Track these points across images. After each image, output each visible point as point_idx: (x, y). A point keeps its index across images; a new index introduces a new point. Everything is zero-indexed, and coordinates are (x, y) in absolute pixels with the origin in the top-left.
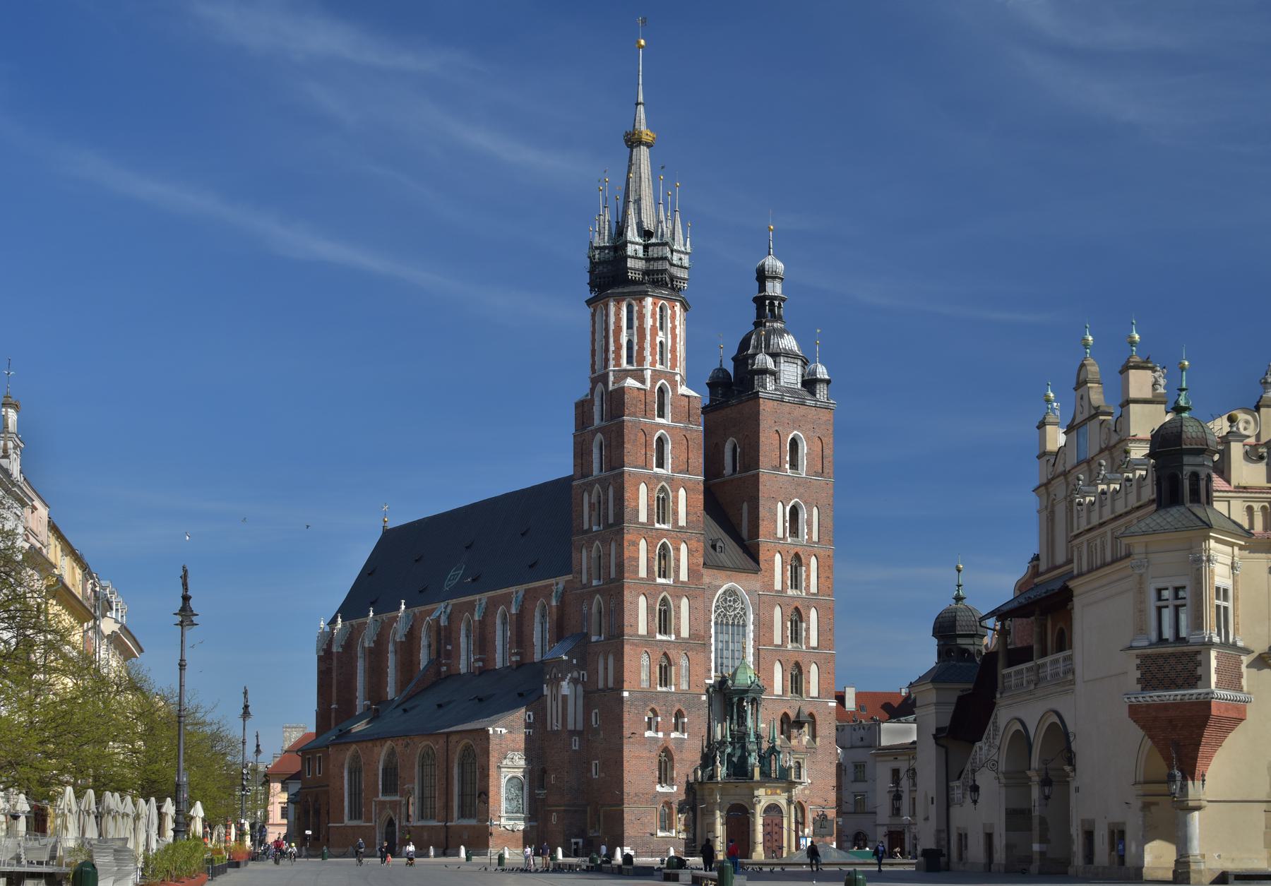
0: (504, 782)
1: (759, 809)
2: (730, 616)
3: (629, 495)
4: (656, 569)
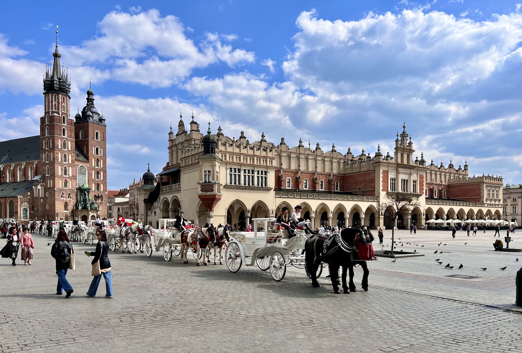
4: (63, 160)
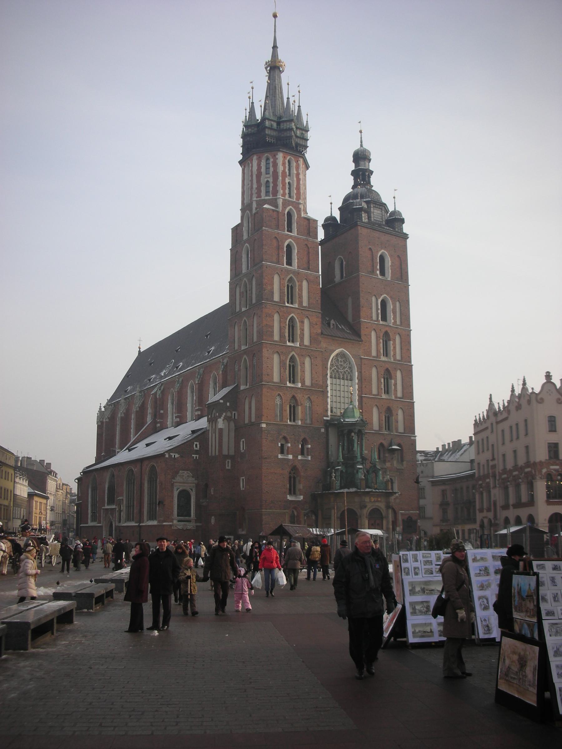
0: (176, 493)
2: (341, 372)
3: (266, 281)
4: (287, 335)
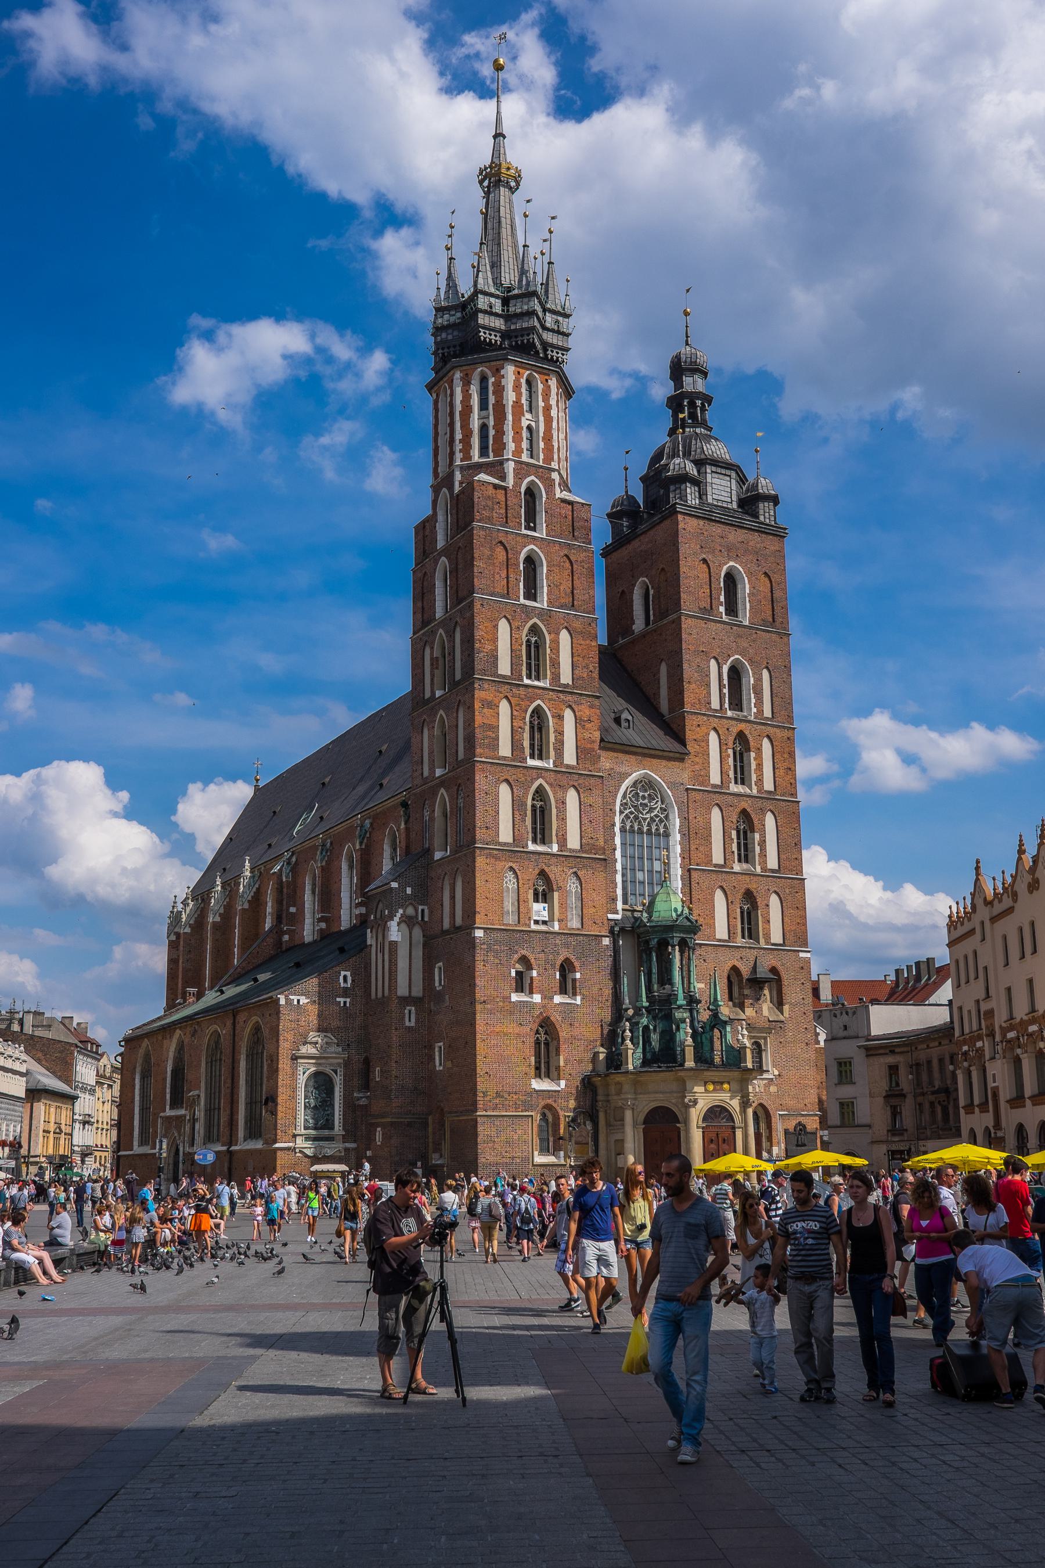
1: (696, 1115)
2: (645, 819)
4: (526, 744)
